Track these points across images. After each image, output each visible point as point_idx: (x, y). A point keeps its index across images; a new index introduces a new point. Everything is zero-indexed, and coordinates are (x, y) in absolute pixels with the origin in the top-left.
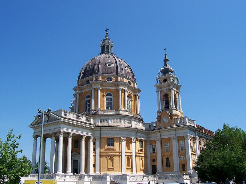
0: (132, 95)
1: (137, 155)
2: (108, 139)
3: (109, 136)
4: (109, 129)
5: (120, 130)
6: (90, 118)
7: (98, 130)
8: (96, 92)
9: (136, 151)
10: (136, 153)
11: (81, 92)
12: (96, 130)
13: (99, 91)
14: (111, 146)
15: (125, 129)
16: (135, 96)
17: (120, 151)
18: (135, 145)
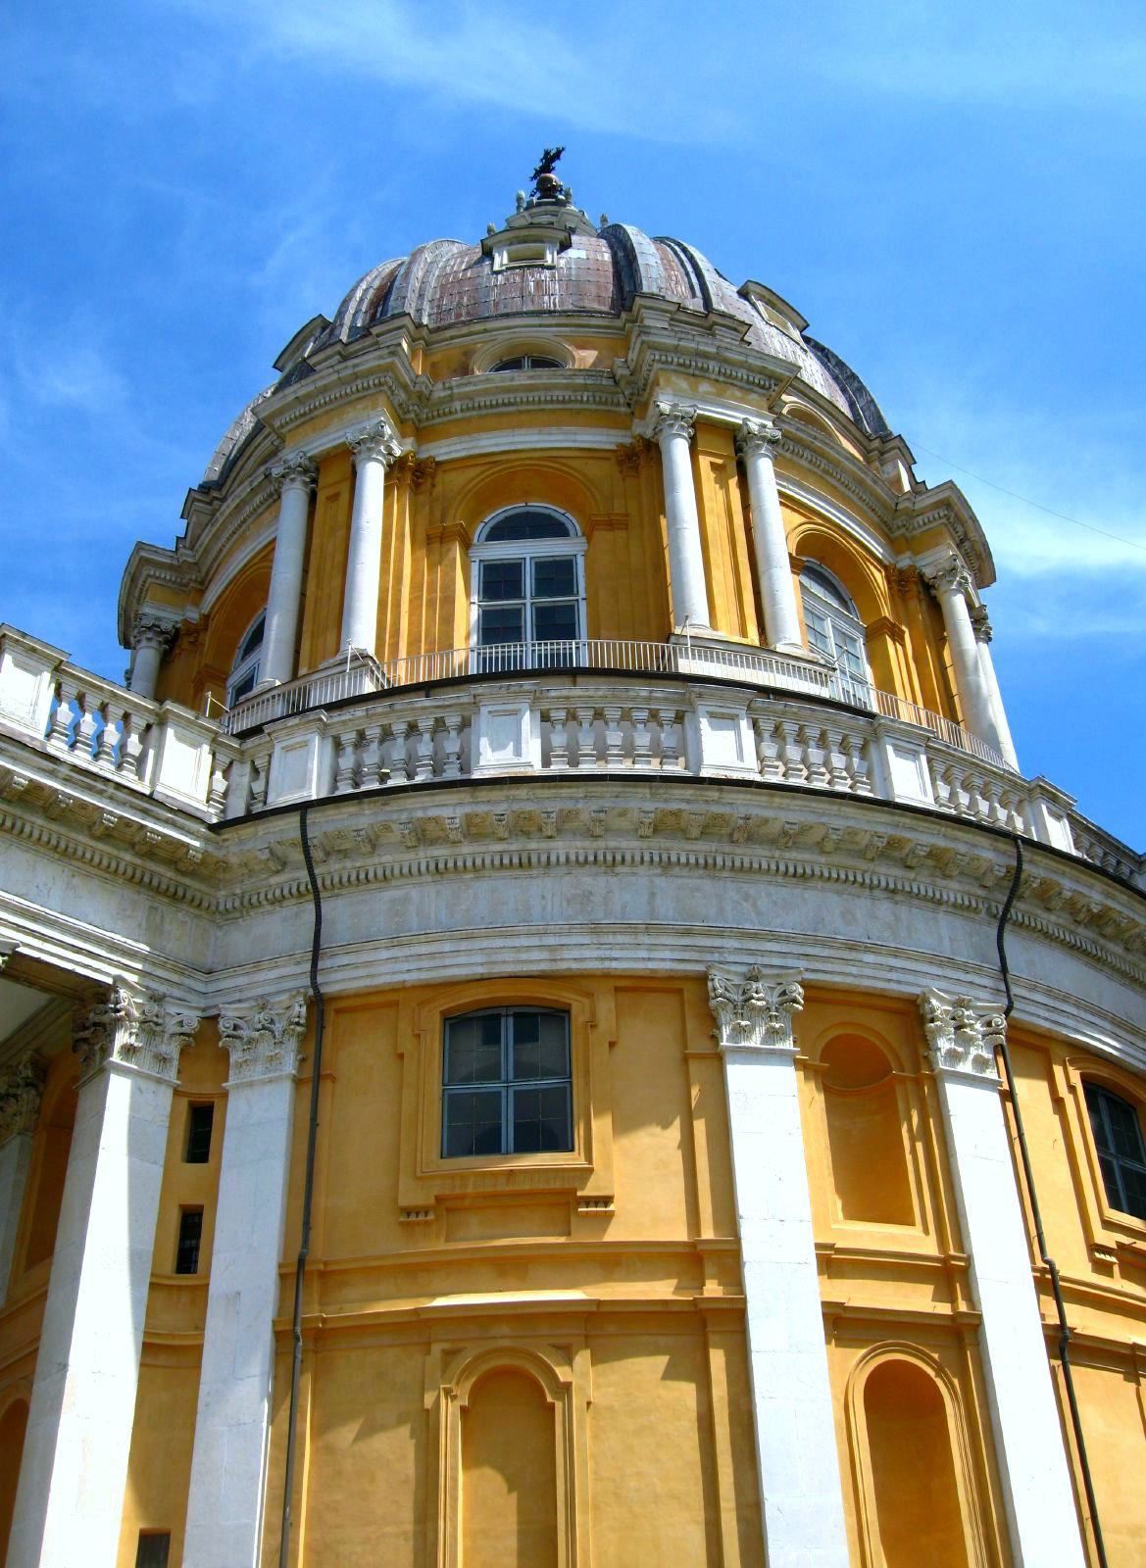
0: (879, 577)
1: (1084, 1320)
2: (473, 1039)
3: (466, 961)
4: (473, 829)
5: (678, 849)
6: (162, 721)
7: (278, 901)
8: (334, 497)
9: (1037, 1239)
10: (1049, 1282)
11: (193, 615)
12: (248, 906)
13: (373, 476)
14: (525, 1145)
15: (787, 838)
16: (914, 589)
17: (708, 1233)
18: (1017, 1138)
